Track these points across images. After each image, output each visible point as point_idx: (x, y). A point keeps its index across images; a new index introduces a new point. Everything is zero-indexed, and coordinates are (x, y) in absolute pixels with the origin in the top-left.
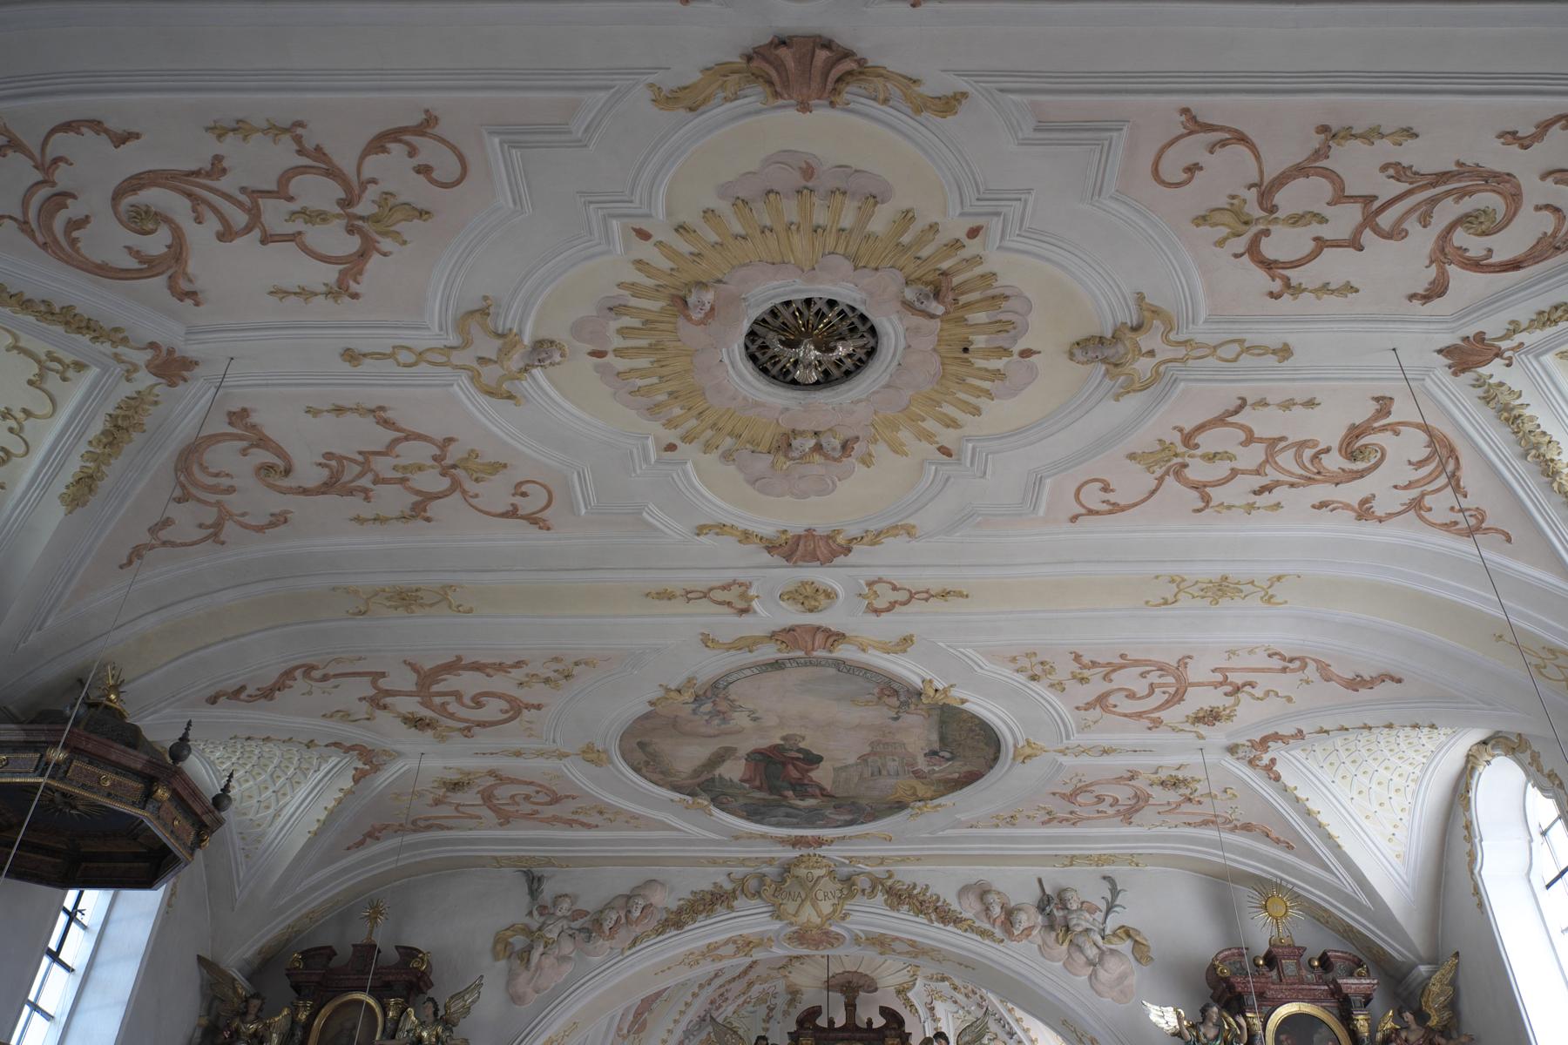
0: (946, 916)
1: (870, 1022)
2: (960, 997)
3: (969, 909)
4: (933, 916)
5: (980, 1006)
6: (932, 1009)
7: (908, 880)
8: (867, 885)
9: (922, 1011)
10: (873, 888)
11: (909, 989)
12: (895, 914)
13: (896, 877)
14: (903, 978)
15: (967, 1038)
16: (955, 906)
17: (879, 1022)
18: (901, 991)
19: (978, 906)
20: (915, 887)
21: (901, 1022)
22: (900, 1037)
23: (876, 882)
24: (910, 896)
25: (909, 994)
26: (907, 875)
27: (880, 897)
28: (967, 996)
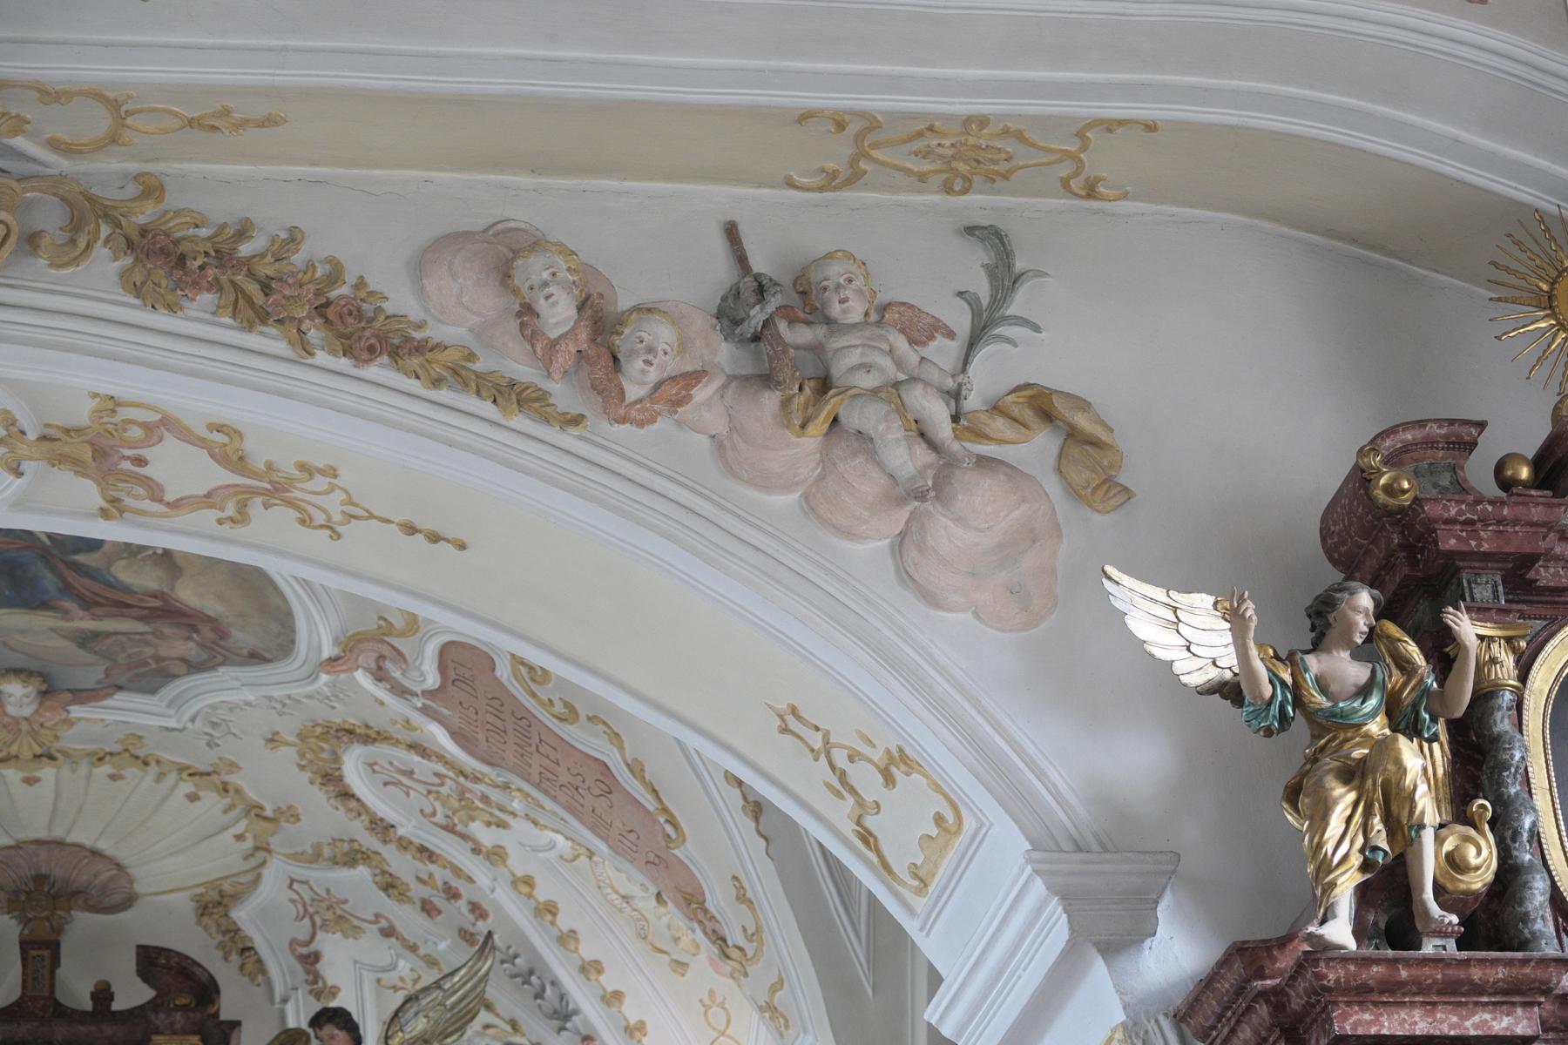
0: (359, 330)
1: (103, 995)
2: (405, 917)
3: (456, 310)
4: (314, 334)
5: (466, 936)
6: (311, 960)
7: (221, 210)
8: (51, 220)
9: (281, 969)
10: (75, 226)
11: (237, 897)
12: (161, 320)
13: (175, 199)
14: (220, 858)
15: (419, 1026)
16: (401, 300)
17: (132, 993)
18: (214, 905)
19: (489, 302)
20: (243, 233)
21: (207, 991)
22: (198, 1029)
23: (86, 215)
24: (223, 256)
25: (241, 915)
26: (213, 186)
27: (105, 265)
28: (428, 908)
